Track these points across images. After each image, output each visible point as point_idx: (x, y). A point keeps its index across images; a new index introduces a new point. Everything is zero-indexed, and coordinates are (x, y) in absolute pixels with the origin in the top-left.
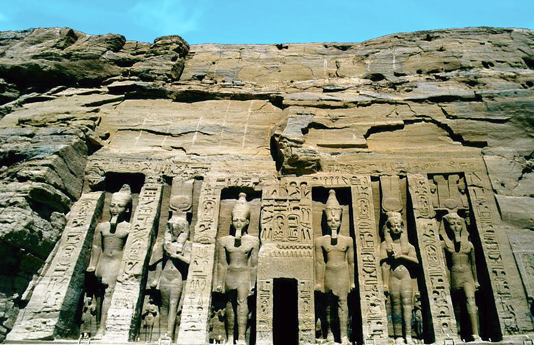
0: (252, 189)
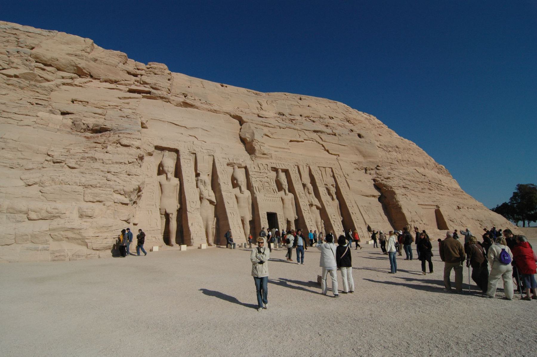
0: (241, 164)
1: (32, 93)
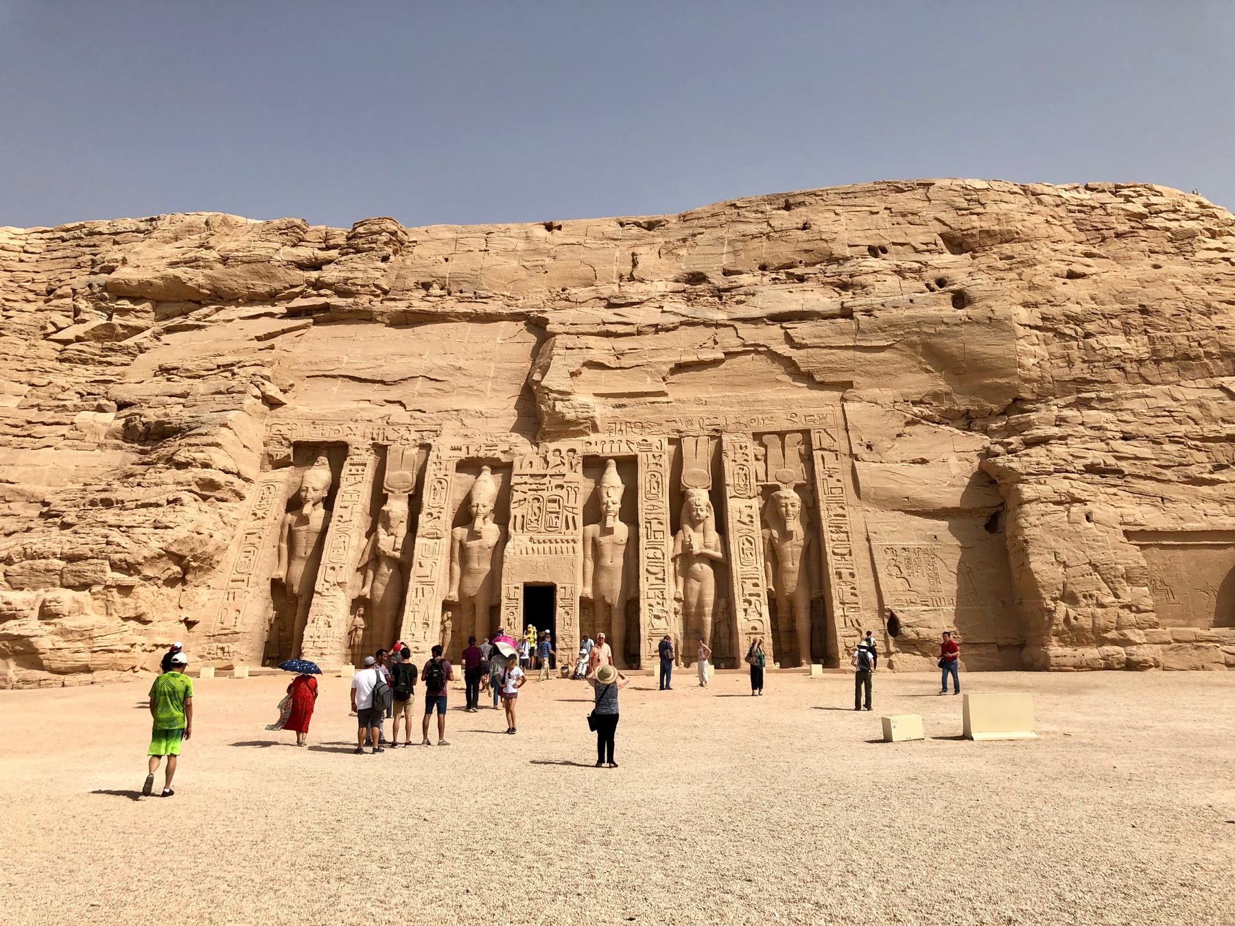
0: (498, 459)
1: (99, 369)
